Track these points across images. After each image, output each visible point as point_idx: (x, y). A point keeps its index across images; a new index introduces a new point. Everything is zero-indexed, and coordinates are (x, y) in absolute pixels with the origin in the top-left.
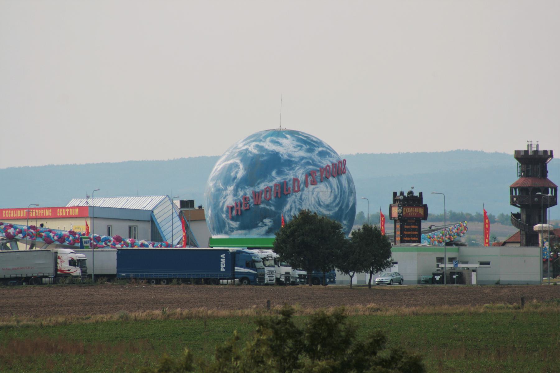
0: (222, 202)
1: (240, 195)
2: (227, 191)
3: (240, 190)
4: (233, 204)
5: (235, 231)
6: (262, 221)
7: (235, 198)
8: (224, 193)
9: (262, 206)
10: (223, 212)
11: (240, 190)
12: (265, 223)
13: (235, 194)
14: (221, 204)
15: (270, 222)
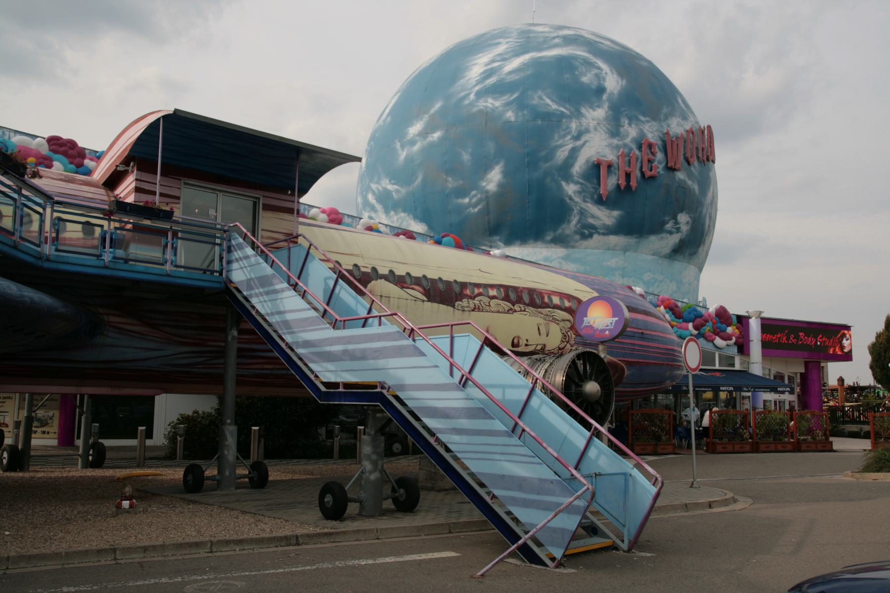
0: (570, 146)
1: (628, 136)
2: (584, 121)
3: (625, 121)
4: (610, 156)
5: (595, 236)
7: (615, 141)
8: (574, 125)
10: (568, 178)
11: (627, 122)
13: (615, 132)
14: (561, 155)
15: (688, 223)
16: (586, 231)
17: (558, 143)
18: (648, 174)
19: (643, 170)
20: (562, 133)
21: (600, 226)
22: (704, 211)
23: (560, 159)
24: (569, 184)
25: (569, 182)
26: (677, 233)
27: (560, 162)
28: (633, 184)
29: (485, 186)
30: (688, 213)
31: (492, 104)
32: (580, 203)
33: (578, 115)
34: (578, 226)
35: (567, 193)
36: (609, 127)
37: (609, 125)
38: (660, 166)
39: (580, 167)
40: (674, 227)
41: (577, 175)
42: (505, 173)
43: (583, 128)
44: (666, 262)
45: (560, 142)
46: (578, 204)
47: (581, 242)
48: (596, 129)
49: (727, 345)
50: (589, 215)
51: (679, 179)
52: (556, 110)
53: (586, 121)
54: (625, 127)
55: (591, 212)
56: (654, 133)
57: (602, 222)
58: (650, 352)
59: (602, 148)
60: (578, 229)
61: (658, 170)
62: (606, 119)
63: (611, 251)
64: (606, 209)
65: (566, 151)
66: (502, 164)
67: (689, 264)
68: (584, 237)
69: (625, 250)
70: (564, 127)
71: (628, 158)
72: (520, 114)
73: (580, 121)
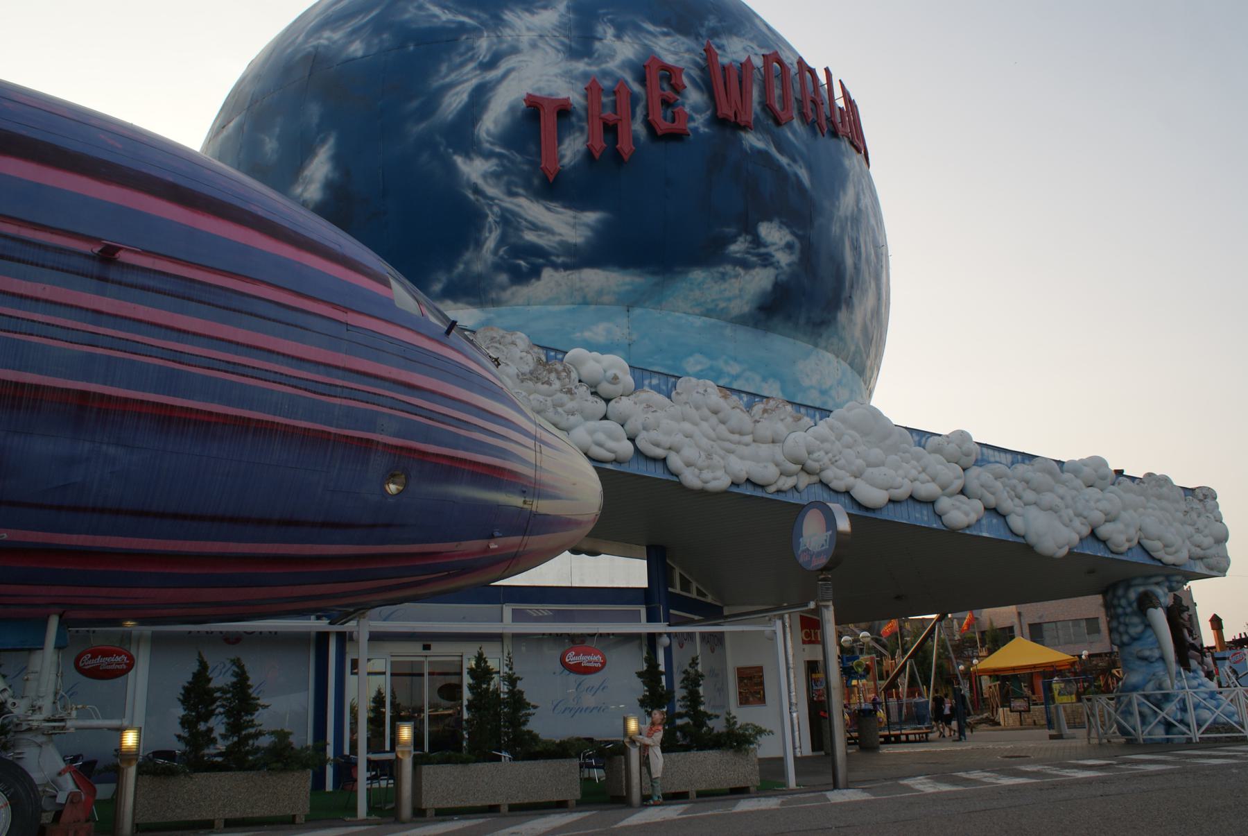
0: (474, 82)
1: (612, 56)
2: (507, 32)
3: (607, 33)
5: (547, 273)
6: (749, 228)
7: (581, 66)
9: (753, 140)
11: (610, 31)
12: (765, 246)
14: (455, 101)
15: (789, 246)
16: (522, 263)
17: (448, 80)
18: (664, 126)
19: (650, 118)
20: (458, 60)
21: (555, 248)
22: (835, 229)
23: (452, 108)
24: (471, 159)
25: (472, 155)
26: (765, 266)
27: (450, 117)
28: (625, 146)
29: (301, 195)
30: (788, 226)
31: (328, 39)
32: (500, 200)
33: (498, 22)
34: (501, 252)
35: (468, 181)
36: (566, 41)
37: (567, 37)
38: (696, 116)
39: (496, 122)
40: (752, 251)
41: (490, 139)
42: (338, 159)
43: (504, 46)
44: (745, 336)
45: (453, 76)
46: (496, 201)
47: (514, 288)
48: (534, 46)
49: (891, 501)
50: (524, 223)
51: (752, 147)
52: (449, 21)
53: (513, 33)
54: (605, 41)
55: (529, 218)
56: (681, 54)
57: (557, 238)
58: (192, 360)
59: (548, 81)
60: (501, 258)
61: (692, 125)
62: (562, 26)
63: (593, 307)
64: (565, 207)
65: (464, 92)
66: (331, 141)
67: (816, 345)
68: (521, 277)
69: (630, 302)
70: (462, 49)
71: (612, 98)
72: (376, 41)
73: (499, 34)
